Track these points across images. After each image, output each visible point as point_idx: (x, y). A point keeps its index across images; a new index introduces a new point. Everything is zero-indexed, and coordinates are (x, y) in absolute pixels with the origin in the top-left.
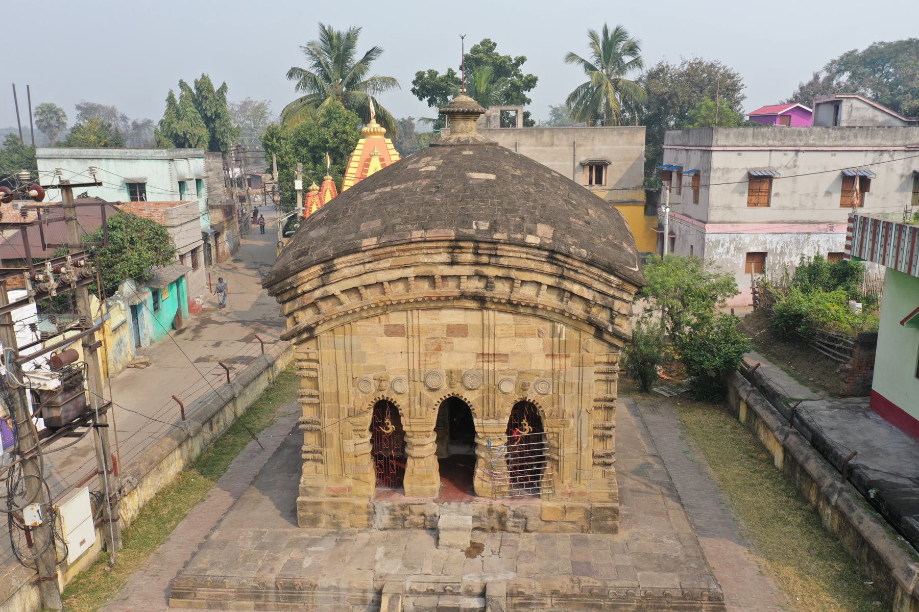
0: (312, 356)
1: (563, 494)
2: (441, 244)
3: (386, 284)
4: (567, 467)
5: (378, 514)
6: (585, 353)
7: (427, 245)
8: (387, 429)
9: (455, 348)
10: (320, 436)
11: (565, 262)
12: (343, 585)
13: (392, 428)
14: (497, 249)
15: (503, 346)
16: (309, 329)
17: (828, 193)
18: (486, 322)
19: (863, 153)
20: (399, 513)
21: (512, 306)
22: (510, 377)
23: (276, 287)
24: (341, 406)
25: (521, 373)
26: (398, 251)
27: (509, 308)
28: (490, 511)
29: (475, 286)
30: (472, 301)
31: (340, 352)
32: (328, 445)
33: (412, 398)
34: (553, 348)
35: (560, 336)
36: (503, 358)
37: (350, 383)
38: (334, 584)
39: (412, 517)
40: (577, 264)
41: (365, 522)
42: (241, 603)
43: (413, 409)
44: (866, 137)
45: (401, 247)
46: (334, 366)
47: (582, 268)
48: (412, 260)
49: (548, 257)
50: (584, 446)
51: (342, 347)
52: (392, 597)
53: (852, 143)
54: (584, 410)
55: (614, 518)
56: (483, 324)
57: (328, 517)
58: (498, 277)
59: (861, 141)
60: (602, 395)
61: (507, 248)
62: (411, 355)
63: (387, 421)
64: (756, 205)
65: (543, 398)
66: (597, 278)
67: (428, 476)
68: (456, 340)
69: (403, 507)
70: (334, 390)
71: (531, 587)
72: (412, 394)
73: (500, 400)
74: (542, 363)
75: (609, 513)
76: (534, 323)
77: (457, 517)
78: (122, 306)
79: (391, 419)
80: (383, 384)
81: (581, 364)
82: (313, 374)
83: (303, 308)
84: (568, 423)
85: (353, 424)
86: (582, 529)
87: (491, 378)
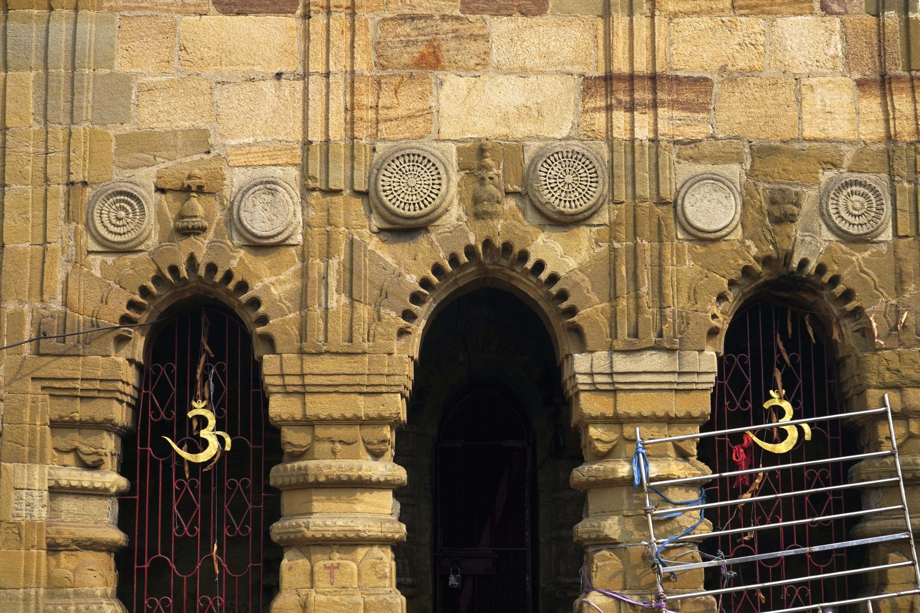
8: (200, 445)
9: (494, 57)
13: (214, 443)
15: (691, 46)
22: (721, 169)
24: (10, 306)
33: (317, 264)
34: (882, 53)
36: (688, 95)
37: (57, 207)
43: (317, 312)
51: (35, 60)
62: (316, 85)
63: (199, 409)
65: (859, 256)
68: (500, 27)
72: (317, 243)
73: (684, 267)
74: (839, 113)
79: (216, 404)
80: (198, 205)
85: (56, 390)
87: (644, 175)
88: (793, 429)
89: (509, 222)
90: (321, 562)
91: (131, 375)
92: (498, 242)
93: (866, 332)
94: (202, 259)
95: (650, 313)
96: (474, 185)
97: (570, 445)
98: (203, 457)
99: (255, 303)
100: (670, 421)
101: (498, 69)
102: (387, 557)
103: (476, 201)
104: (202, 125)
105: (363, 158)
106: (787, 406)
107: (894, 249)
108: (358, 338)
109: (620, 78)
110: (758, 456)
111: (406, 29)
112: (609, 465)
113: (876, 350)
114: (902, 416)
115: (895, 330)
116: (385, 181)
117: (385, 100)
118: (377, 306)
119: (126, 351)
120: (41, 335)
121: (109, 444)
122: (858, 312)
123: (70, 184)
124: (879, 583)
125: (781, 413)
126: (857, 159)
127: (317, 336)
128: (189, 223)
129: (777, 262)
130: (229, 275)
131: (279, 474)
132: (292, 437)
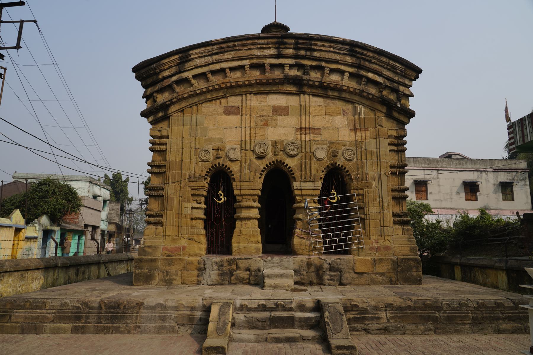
0: (164, 133)
1: (371, 249)
2: (271, 40)
3: (228, 71)
4: (373, 224)
5: (207, 270)
6: (380, 128)
7: (260, 41)
9: (279, 124)
10: (162, 203)
11: (362, 54)
12: (170, 304)
13: (223, 199)
14: (312, 44)
15: (317, 122)
16: (165, 107)
17: (458, 193)
18: (303, 103)
19: (472, 172)
20: (226, 268)
21: (324, 90)
22: (323, 146)
23: (143, 71)
24: (184, 172)
25: (331, 143)
26: (239, 45)
27: (320, 92)
28: (309, 264)
29: (295, 72)
30: (292, 86)
31: (187, 128)
32: (169, 208)
33: (243, 164)
35: (360, 114)
36: (316, 132)
37: (193, 153)
38: (162, 302)
39: (238, 272)
40: (370, 54)
41: (195, 279)
42: (58, 325)
43: (243, 174)
44: (472, 164)
45: (240, 43)
46: (181, 139)
47: (374, 58)
48: (248, 53)
49: (349, 50)
50: (386, 204)
51: (189, 124)
52: (223, 306)
53: (465, 167)
54: (383, 173)
55: (417, 268)
56: (301, 105)
57: (161, 274)
58: (312, 68)
59: (470, 166)
60: (395, 162)
61: (319, 43)
62: (243, 129)
63: (220, 192)
64: (420, 199)
65: (350, 164)
66: (386, 66)
67: (254, 236)
68: (280, 118)
69: (231, 262)
70: (179, 159)
71: (364, 302)
73: (315, 165)
74: (346, 136)
75: (413, 263)
76: (340, 105)
77: (280, 271)
78: (38, 228)
79: (223, 191)
80: (220, 153)
81: (377, 137)
82: (163, 148)
83: (161, 91)
84: (371, 184)
85: (193, 188)
86: (391, 281)
87: (307, 147)
88: (336, 197)
89: (281, 156)
90: (244, 222)
91: (207, 185)
92: (279, 160)
93: (351, 178)
94: (221, 163)
95: (308, 174)
96: (274, 149)
97: (293, 200)
98: (221, 202)
99: (231, 172)
100: (312, 196)
101: (279, 126)
102: (257, 221)
103: (275, 152)
104: (221, 137)
105: (252, 143)
106: (335, 193)
107: (357, 162)
108: (251, 179)
109: (303, 128)
110: (330, 203)
111: (261, 118)
112: (300, 204)
113: (353, 182)
114: (358, 195)
115: (357, 178)
116: (257, 148)
117: (257, 132)
118: (255, 172)
119: (206, 181)
120: (190, 178)
121: (203, 199)
122: (350, 175)
123: (196, 148)
124: (353, 228)
125: (334, 194)
126: (350, 145)
127: (243, 178)
128: (219, 156)
129: (334, 165)
130: (226, 166)
131: (236, 205)
132: (238, 198)
